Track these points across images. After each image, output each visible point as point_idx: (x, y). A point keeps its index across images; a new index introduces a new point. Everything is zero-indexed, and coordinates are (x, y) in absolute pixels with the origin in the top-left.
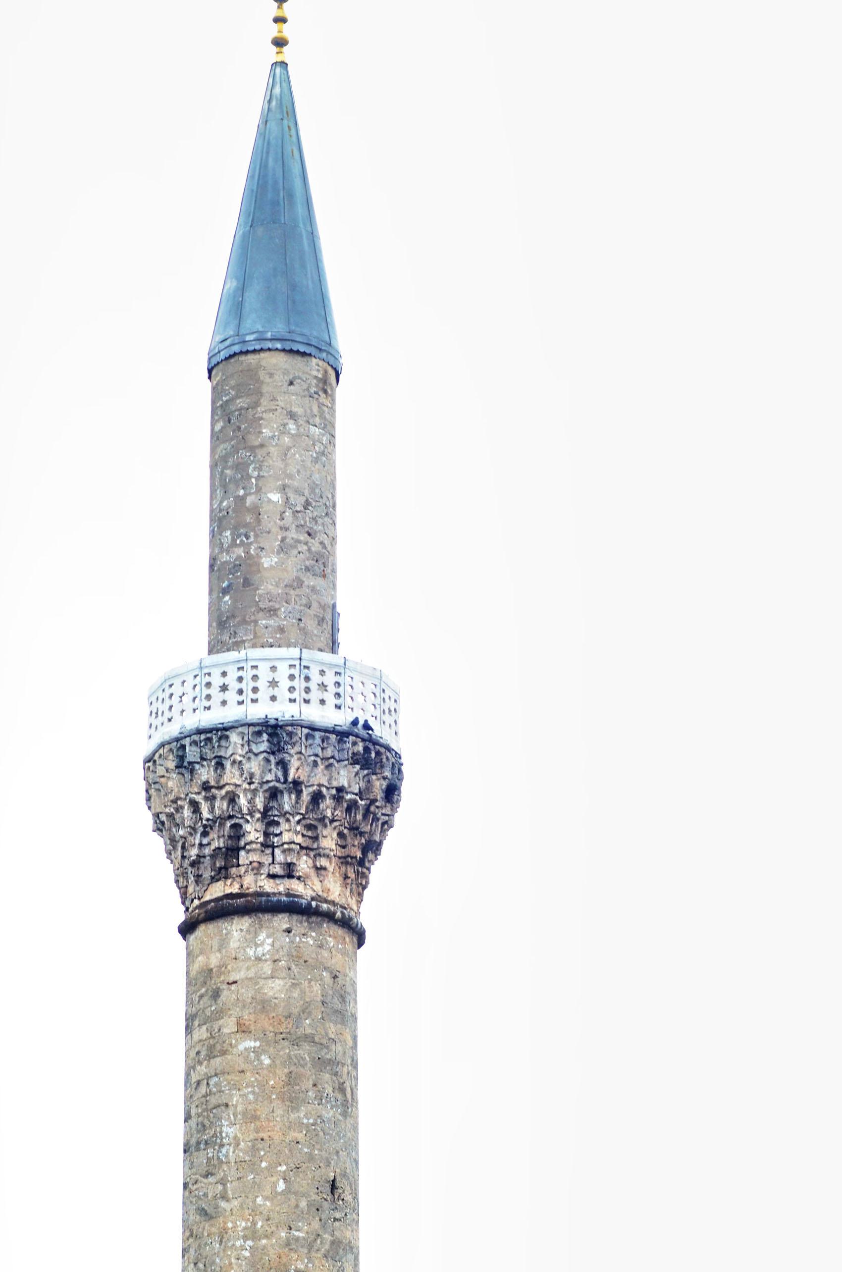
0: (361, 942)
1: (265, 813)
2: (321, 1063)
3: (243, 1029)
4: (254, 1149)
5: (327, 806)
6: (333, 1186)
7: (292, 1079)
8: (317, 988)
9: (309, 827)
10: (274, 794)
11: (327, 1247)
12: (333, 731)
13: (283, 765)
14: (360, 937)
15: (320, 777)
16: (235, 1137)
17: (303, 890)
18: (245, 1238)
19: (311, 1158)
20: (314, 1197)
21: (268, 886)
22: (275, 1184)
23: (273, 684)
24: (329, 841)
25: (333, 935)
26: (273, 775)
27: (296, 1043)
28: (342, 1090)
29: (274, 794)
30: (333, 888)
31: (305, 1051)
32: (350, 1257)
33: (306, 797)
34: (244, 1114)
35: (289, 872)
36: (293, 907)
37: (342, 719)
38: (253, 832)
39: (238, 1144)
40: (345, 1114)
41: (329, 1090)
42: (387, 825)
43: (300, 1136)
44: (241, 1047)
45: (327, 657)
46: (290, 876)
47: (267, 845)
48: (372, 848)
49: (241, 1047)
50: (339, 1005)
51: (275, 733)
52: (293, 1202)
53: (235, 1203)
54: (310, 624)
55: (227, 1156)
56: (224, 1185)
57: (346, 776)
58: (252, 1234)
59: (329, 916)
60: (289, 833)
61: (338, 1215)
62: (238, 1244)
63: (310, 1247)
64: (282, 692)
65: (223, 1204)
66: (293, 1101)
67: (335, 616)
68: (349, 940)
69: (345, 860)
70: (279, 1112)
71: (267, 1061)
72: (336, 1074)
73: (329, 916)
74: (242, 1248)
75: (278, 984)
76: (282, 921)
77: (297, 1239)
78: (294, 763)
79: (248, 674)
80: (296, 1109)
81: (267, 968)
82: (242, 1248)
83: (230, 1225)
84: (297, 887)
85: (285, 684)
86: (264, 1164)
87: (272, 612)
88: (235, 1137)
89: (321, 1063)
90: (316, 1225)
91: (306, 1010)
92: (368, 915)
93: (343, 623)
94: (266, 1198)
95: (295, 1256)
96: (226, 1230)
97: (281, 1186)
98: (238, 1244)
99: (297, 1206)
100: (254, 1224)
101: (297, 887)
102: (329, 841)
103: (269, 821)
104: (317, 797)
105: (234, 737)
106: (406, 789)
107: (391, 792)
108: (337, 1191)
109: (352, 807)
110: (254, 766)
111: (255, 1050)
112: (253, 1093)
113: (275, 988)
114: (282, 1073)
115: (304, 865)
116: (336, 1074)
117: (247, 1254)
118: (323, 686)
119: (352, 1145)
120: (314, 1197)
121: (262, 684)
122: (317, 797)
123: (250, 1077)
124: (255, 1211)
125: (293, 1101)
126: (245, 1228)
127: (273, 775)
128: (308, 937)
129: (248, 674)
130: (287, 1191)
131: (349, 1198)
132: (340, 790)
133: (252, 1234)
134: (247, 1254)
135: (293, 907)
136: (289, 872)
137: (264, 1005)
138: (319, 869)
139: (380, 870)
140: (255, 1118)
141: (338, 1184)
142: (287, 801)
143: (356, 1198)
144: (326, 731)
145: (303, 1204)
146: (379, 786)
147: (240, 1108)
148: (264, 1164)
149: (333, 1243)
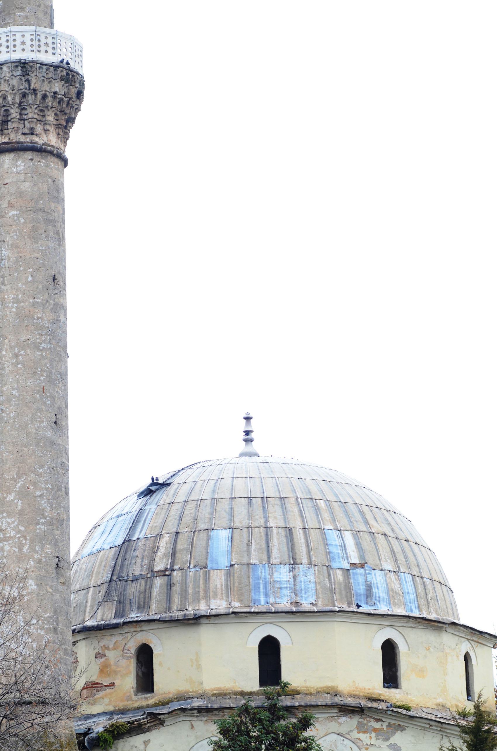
0: (66, 165)
1: (20, 104)
2: (48, 221)
3: (11, 206)
4: (17, 262)
5: (49, 101)
6: (54, 278)
7: (34, 229)
8: (45, 186)
9: (41, 111)
10: (24, 95)
11: (52, 306)
12: (52, 65)
13: (28, 81)
14: (65, 162)
15: (46, 87)
16: (8, 256)
17: (39, 141)
18: (13, 303)
19: (44, 265)
20: (45, 283)
21: (22, 139)
22: (27, 278)
23: (23, 43)
24: (50, 118)
25: (53, 162)
26: (24, 86)
27: (36, 212)
28: (58, 233)
29: (24, 95)
30: (52, 139)
31: (40, 216)
32: (63, 311)
33: (39, 96)
34: (12, 245)
35: (32, 132)
36: (34, 149)
37: (55, 60)
38: (14, 113)
39: (9, 259)
40: (59, 245)
41: (52, 234)
42: (78, 110)
43: (39, 255)
44: (10, 214)
45: (48, 30)
48: (71, 121)
49: (10, 214)
50: (56, 193)
51: (24, 66)
52: (35, 286)
53: (9, 286)
54: (40, 15)
55: (4, 265)
56: (3, 278)
57: (58, 87)
58: (17, 300)
59: (51, 153)
60: (32, 113)
61: (57, 292)
62: (10, 305)
63: (44, 306)
64: (27, 47)
65: (3, 287)
66: (35, 239)
67: (52, 11)
68: (60, 164)
69: (58, 126)
70: (29, 244)
71: (22, 221)
72: (55, 226)
73: (51, 153)
74: (12, 307)
75: (27, 184)
76: (29, 155)
77: (38, 303)
78: (33, 81)
79: (11, 38)
80: (36, 242)
81: (22, 177)
82: (12, 307)
83: (6, 297)
84: (36, 139)
85: (29, 43)
86: (22, 268)
87: (22, 9)
88: (8, 256)
89: (48, 221)
90: (46, 296)
91: (41, 196)
92: (69, 152)
93: (55, 15)
94: (23, 284)
95: (37, 311)
96: (4, 299)
97: (30, 278)
98: (10, 305)
99: (37, 288)
100: (18, 296)
101: (36, 139)
102: (50, 118)
103: (22, 107)
104: (44, 97)
105: (5, 68)
106: (87, 93)
107: (80, 94)
108: (56, 281)
109: (60, 101)
110: (15, 82)
111: (17, 216)
112: (16, 235)
113: (26, 186)
114: (30, 226)
115: (39, 129)
116: (55, 226)
117: (14, 310)
118: (47, 44)
119: (62, 259)
120: (45, 283)
121: (18, 43)
122: (44, 97)
123: (15, 228)
124: (18, 290)
125: (35, 239)
126: (13, 298)
127: (24, 86)
128: (41, 162)
129: (11, 38)
130: (33, 281)
131: (61, 284)
132: (55, 93)
133: (17, 300)
134: (14, 310)
135: (34, 149)
136: (32, 132)
137: (21, 194)
138: (46, 131)
139: (74, 131)
140: (17, 247)
141: (56, 277)
142: (30, 98)
143: (65, 284)
144: (48, 65)
145: (40, 287)
146: (73, 91)
147: (10, 243)
148: (22, 268)
149: (54, 304)
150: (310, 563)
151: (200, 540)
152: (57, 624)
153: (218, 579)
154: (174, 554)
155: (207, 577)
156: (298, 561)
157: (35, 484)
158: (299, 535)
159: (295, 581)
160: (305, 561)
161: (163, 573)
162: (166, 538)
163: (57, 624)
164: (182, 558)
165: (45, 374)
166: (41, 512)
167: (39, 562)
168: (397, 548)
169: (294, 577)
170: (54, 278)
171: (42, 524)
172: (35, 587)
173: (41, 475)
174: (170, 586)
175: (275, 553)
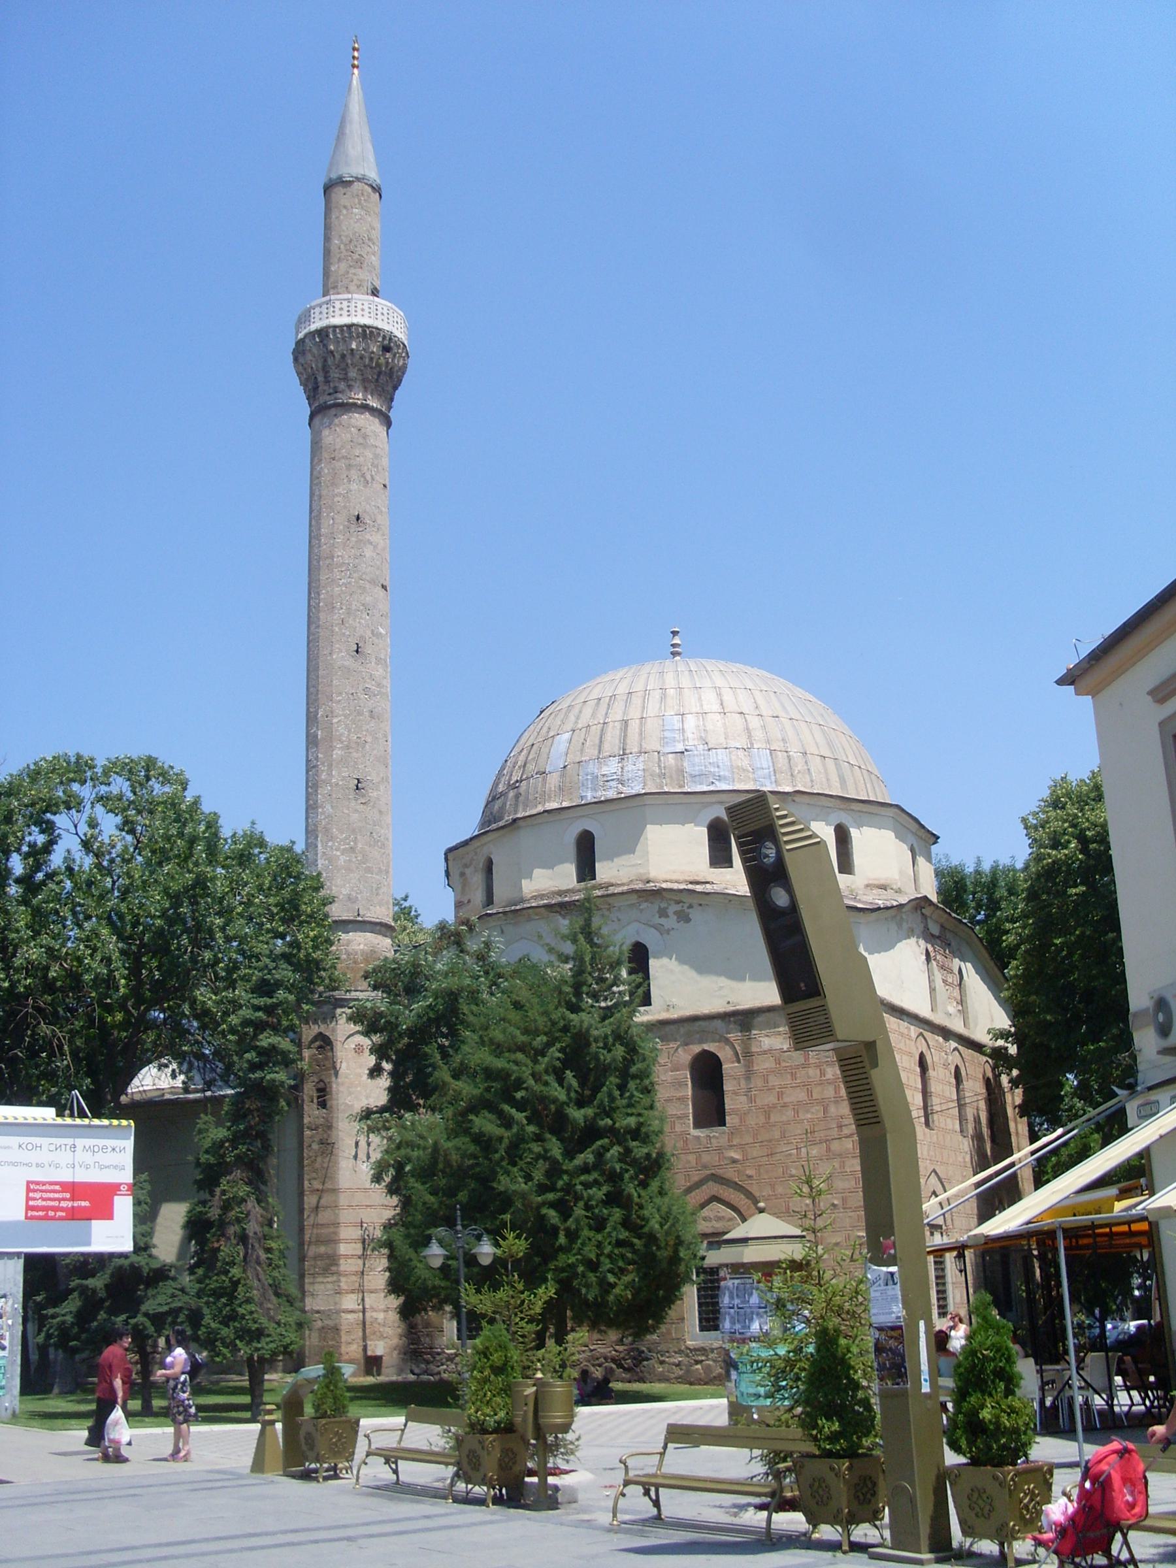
6: (358, 518)
38: (320, 379)
47: (327, 382)
102: (353, 373)
104: (343, 356)
122: (343, 356)
142: (330, 361)
151: (545, 750)
153: (553, 780)
154: (525, 766)
155: (544, 780)
158: (634, 726)
162: (525, 752)
164: (531, 767)
168: (755, 722)
170: (358, 518)
174: (517, 796)
175: (607, 747)
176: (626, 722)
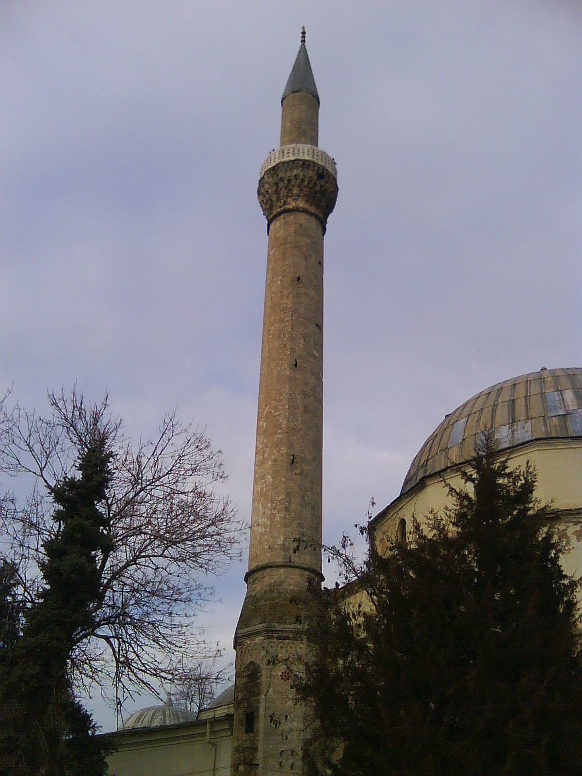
6: (299, 279)
10: (277, 184)
15: (288, 174)
24: (295, 191)
29: (277, 184)
33: (286, 182)
38: (274, 198)
46: (285, 205)
60: (283, 193)
76: (283, 216)
102: (295, 191)
104: (289, 181)
122: (289, 181)
127: (275, 179)
132: (296, 175)
142: (281, 184)
150: (528, 418)
152: (290, 504)
156: (516, 420)
157: (275, 408)
158: (520, 404)
159: (513, 434)
160: (523, 418)
161: (423, 466)
163: (290, 504)
165: (286, 336)
166: (279, 426)
167: (275, 461)
169: (513, 432)
171: (279, 433)
172: (271, 479)
173: (279, 401)
176: (513, 401)
